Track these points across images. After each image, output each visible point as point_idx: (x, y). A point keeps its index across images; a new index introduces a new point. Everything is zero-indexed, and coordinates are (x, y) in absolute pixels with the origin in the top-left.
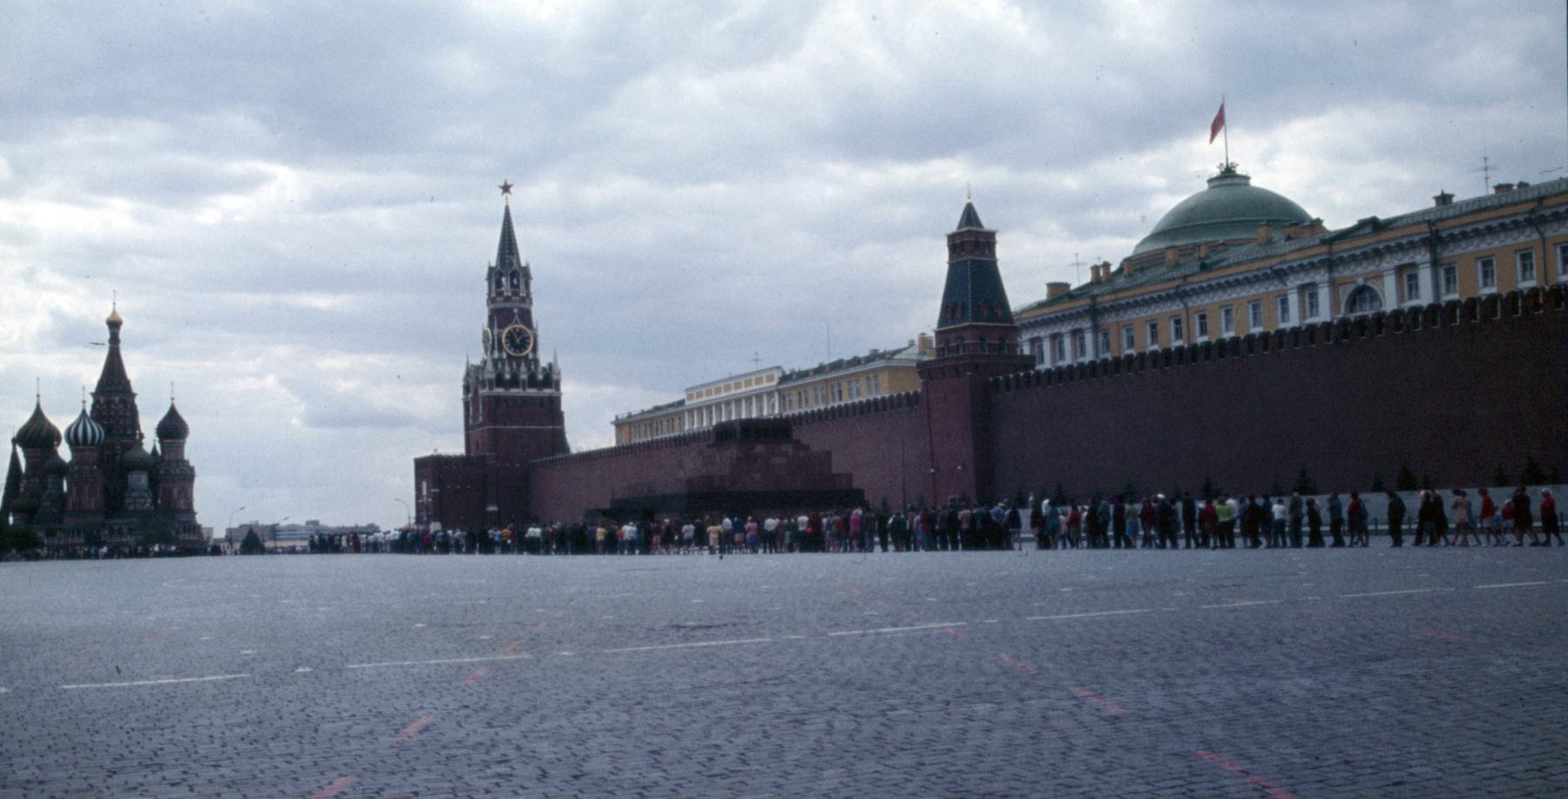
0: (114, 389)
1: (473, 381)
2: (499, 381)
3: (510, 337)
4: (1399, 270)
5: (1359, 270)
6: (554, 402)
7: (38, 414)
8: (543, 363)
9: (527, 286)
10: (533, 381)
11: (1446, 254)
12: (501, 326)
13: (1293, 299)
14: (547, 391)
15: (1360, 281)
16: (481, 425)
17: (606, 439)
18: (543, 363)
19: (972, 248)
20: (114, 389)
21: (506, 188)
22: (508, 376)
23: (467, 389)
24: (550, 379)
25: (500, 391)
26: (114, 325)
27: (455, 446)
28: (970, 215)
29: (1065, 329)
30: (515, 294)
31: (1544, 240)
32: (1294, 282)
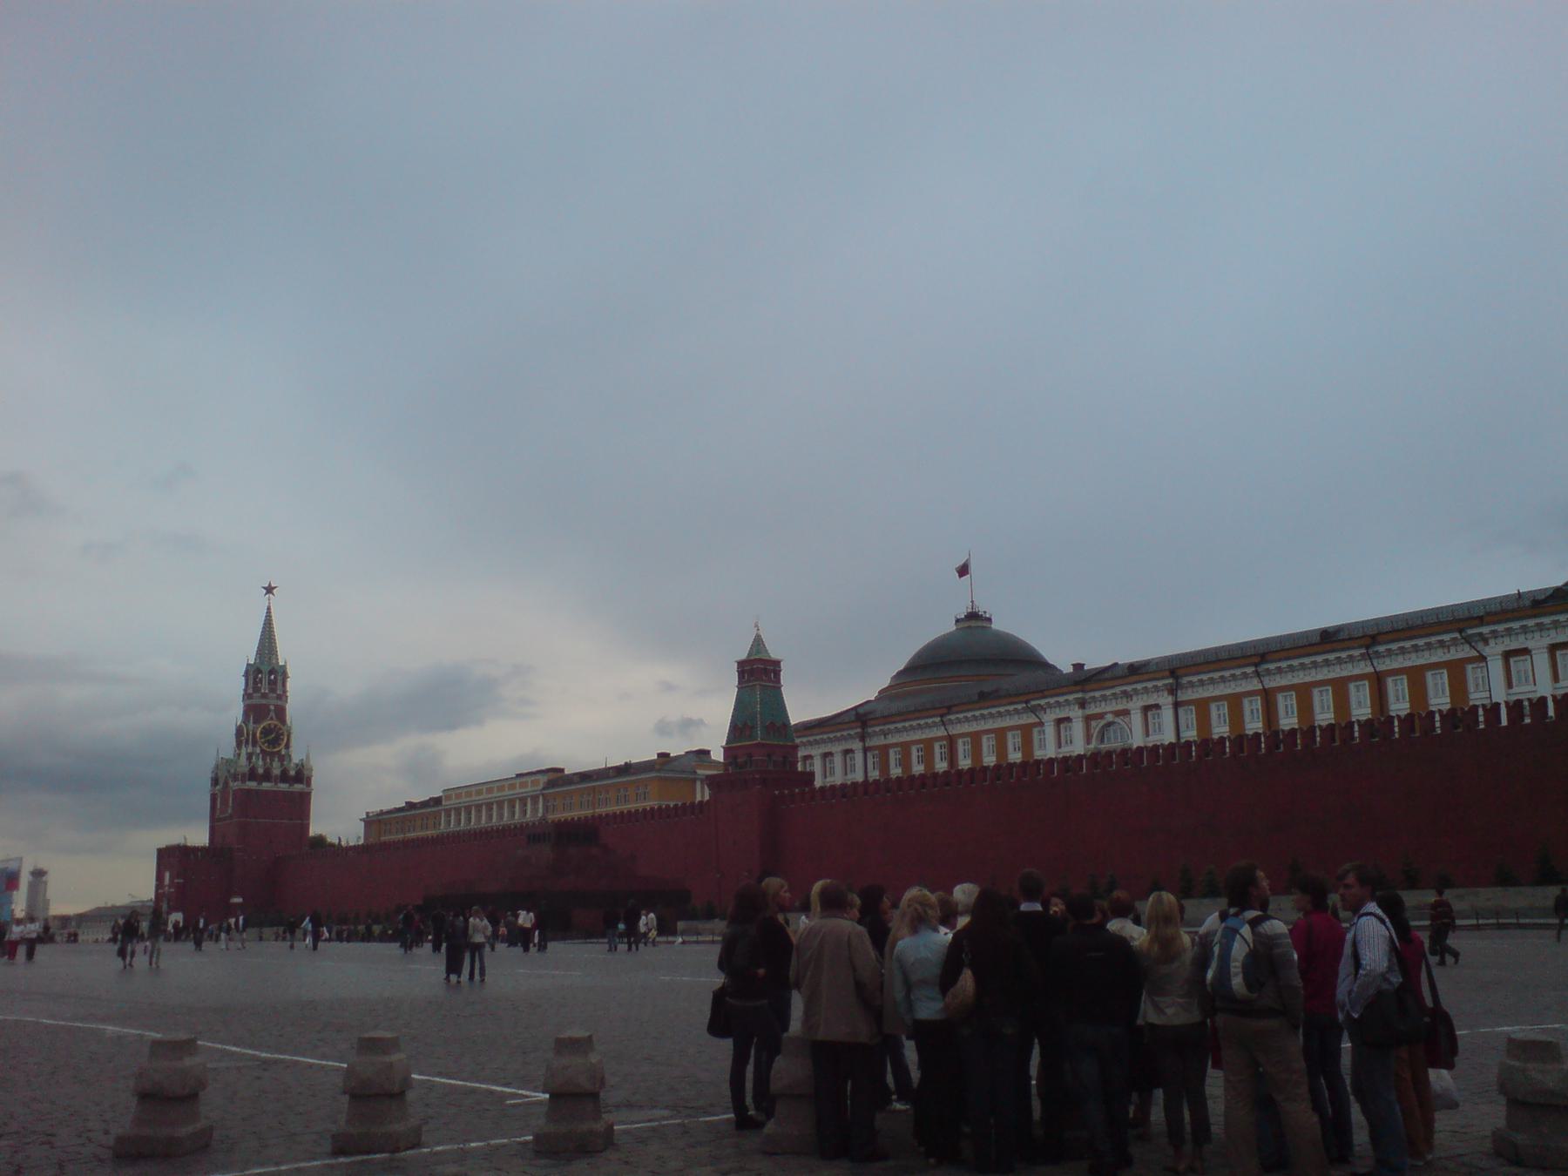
2: (252, 774)
3: (266, 732)
6: (303, 800)
8: (296, 759)
9: (284, 685)
10: (284, 777)
14: (298, 787)
15: (1110, 718)
16: (231, 817)
18: (296, 759)
19: (759, 673)
21: (269, 590)
22: (261, 771)
23: (215, 781)
25: (252, 785)
27: (198, 836)
29: (837, 748)
30: (273, 690)
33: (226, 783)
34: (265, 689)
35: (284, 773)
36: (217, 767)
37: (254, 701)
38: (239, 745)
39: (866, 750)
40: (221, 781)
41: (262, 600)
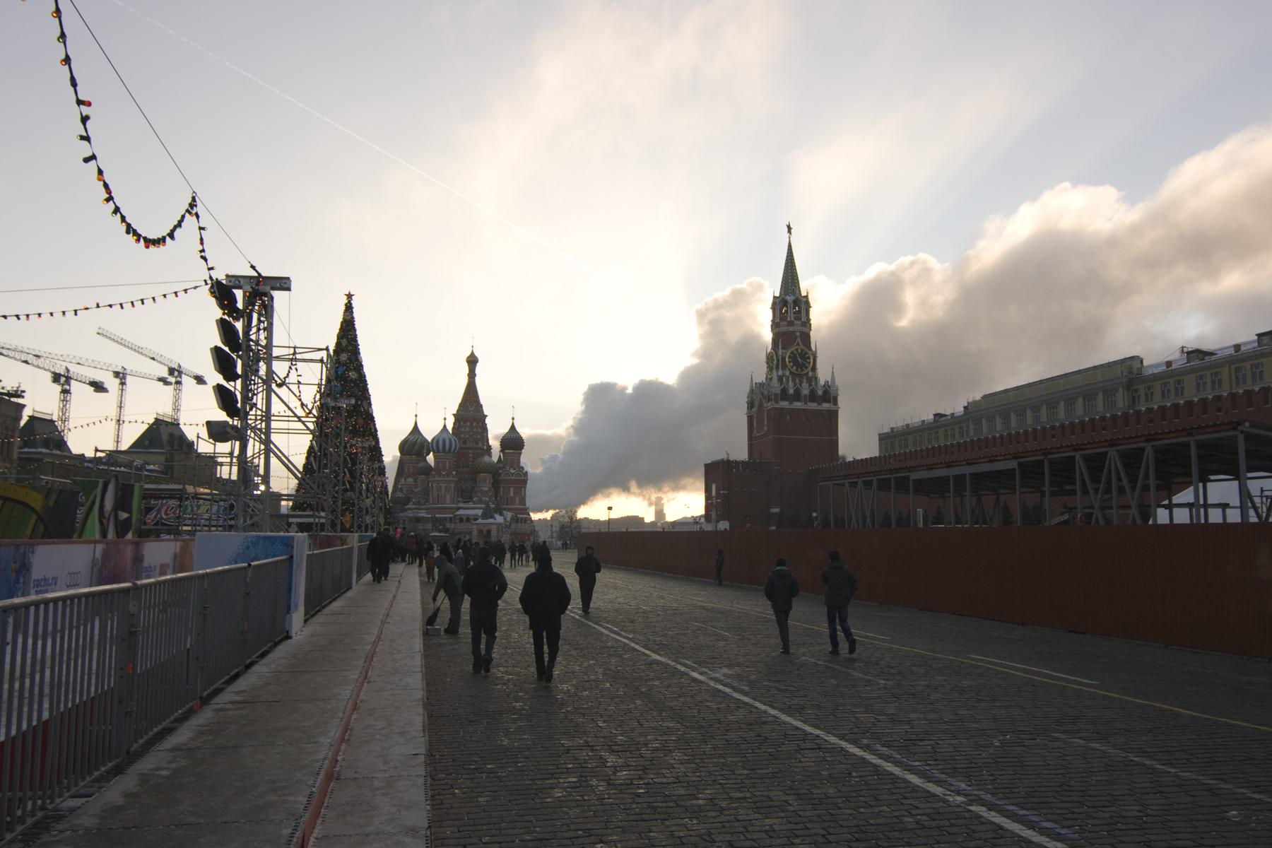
0: (471, 410)
1: (758, 400)
2: (784, 395)
3: (793, 358)
6: (832, 417)
7: (416, 428)
10: (813, 397)
14: (826, 406)
18: (822, 383)
20: (471, 410)
22: (791, 391)
23: (751, 405)
24: (829, 395)
25: (785, 404)
26: (472, 361)
27: (740, 452)
33: (761, 405)
34: (791, 317)
35: (813, 392)
36: (752, 391)
37: (784, 329)
38: (770, 368)
40: (756, 404)
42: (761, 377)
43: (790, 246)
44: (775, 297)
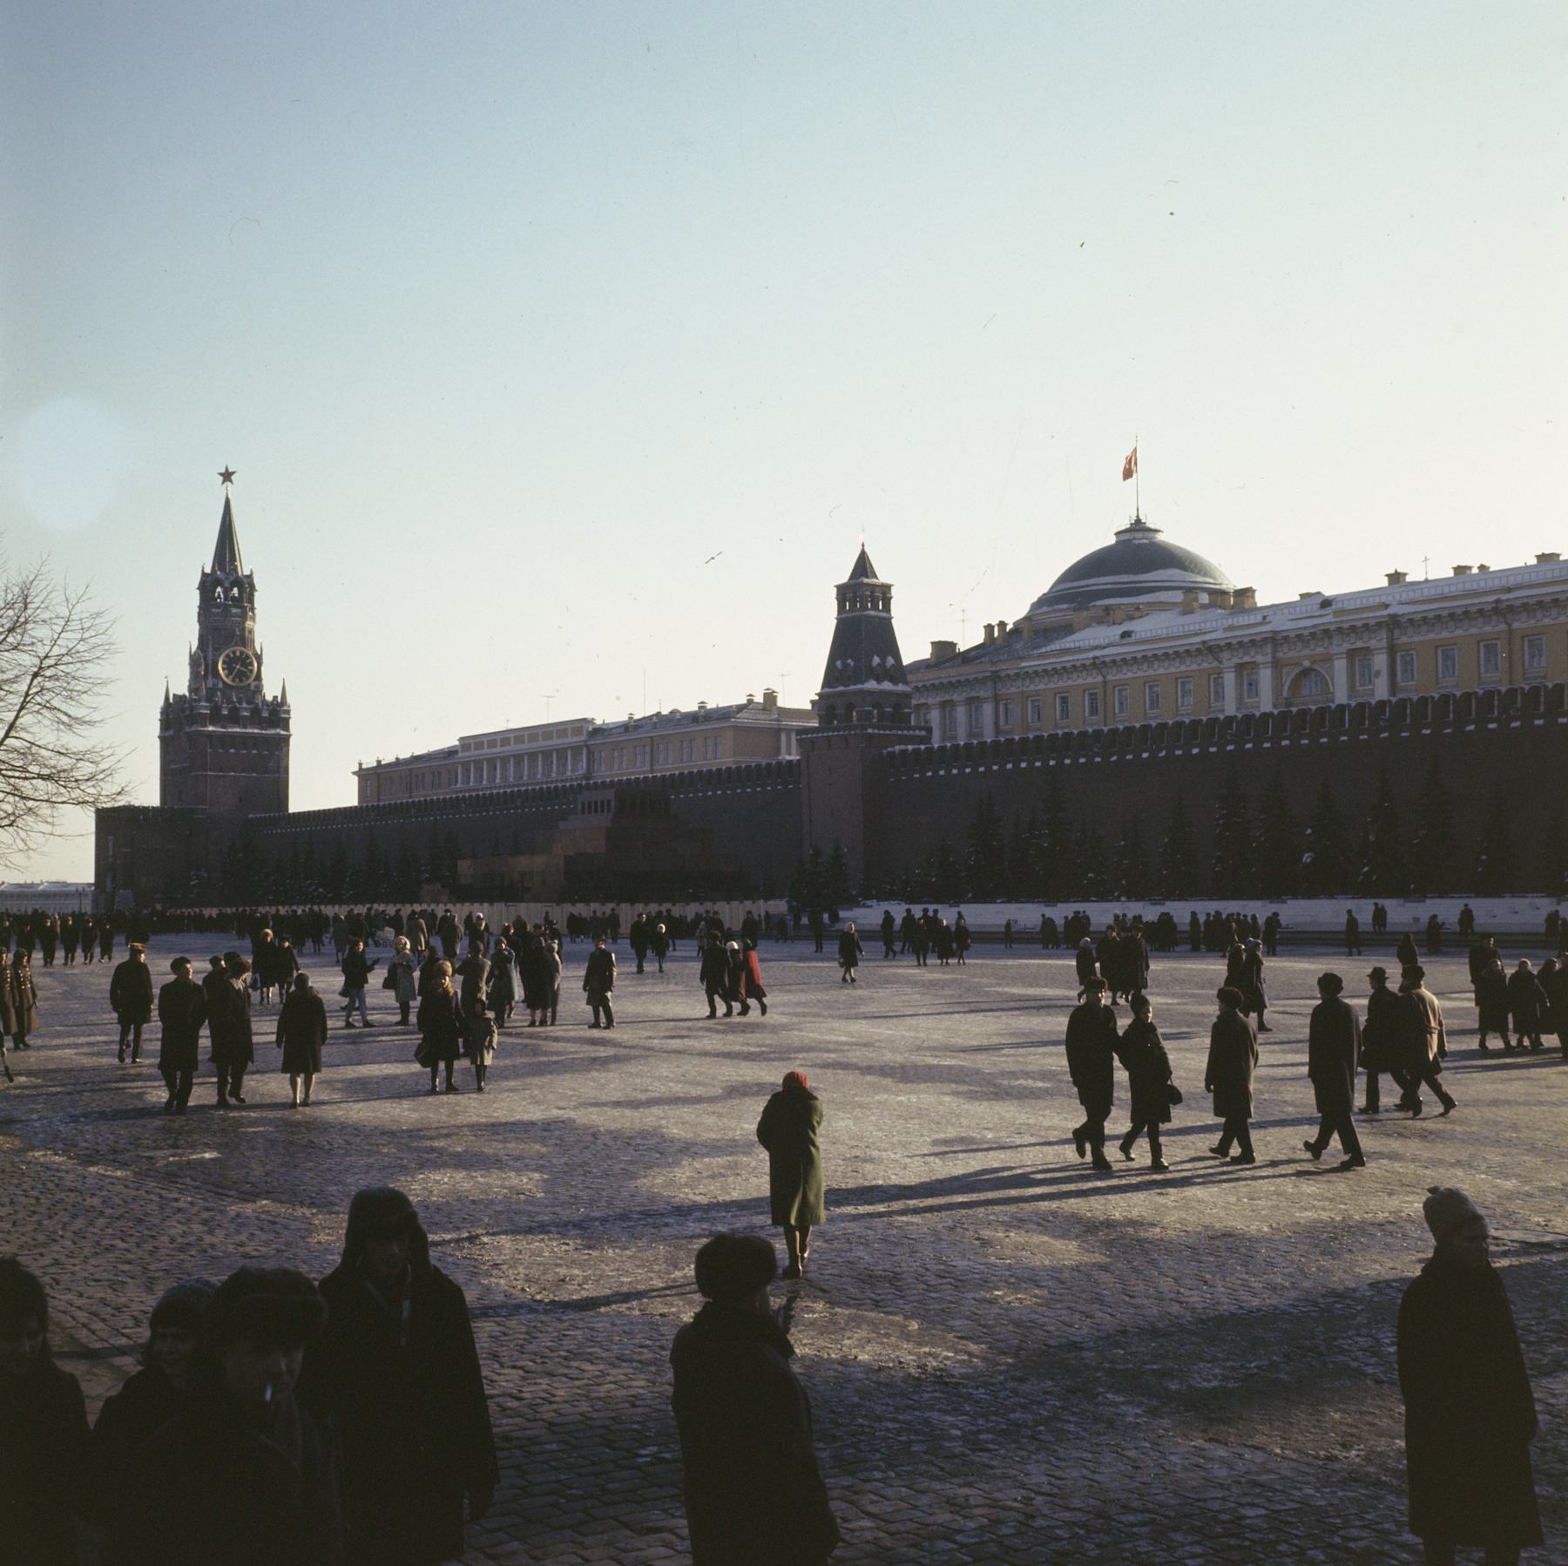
4: (1351, 654)
5: (1306, 652)
8: (269, 698)
10: (256, 718)
11: (1404, 639)
12: (218, 651)
13: (1229, 678)
15: (1307, 664)
17: (348, 797)
18: (269, 698)
21: (227, 476)
24: (277, 714)
27: (148, 794)
28: (863, 566)
31: (1510, 631)
32: (1230, 660)
35: (256, 712)
39: (996, 699)
41: (219, 491)
42: (181, 687)
43: (227, 502)
44: (204, 575)
